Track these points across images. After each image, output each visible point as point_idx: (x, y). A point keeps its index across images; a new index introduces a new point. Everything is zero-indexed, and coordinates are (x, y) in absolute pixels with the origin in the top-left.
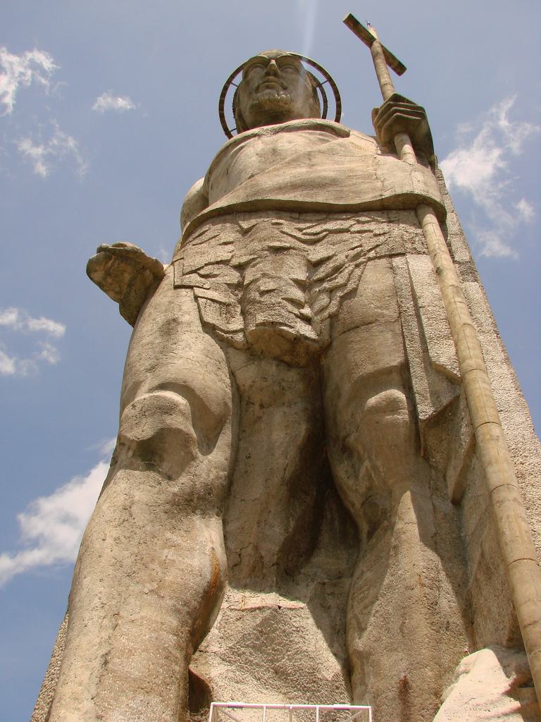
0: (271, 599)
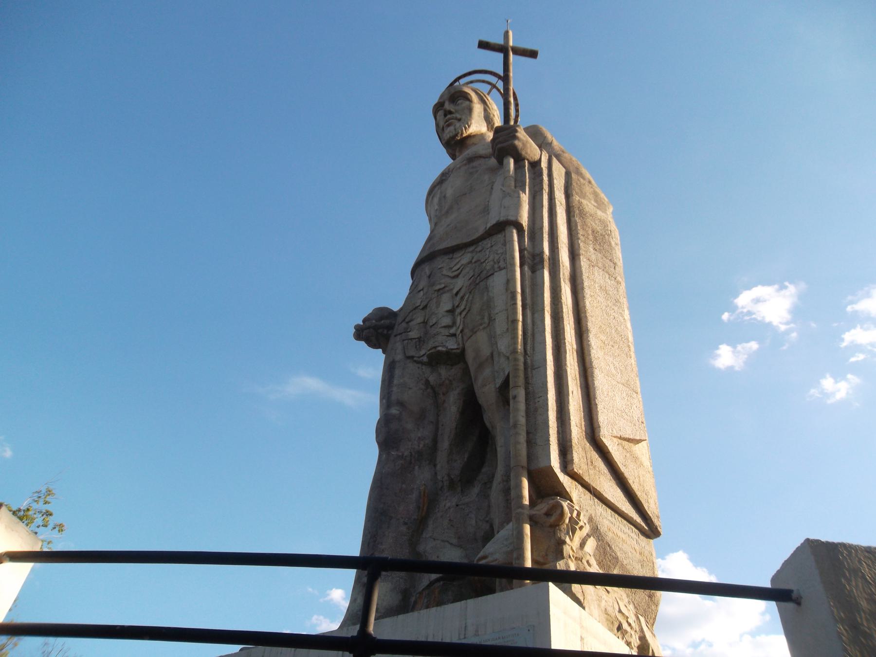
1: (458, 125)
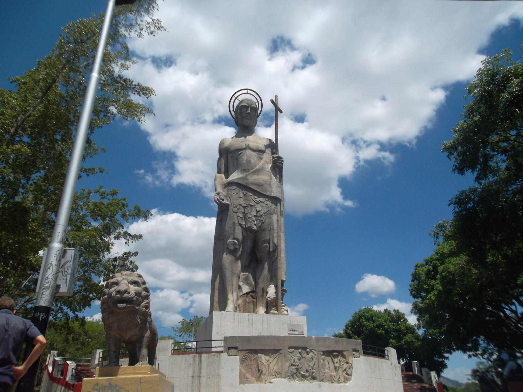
0: (247, 273)
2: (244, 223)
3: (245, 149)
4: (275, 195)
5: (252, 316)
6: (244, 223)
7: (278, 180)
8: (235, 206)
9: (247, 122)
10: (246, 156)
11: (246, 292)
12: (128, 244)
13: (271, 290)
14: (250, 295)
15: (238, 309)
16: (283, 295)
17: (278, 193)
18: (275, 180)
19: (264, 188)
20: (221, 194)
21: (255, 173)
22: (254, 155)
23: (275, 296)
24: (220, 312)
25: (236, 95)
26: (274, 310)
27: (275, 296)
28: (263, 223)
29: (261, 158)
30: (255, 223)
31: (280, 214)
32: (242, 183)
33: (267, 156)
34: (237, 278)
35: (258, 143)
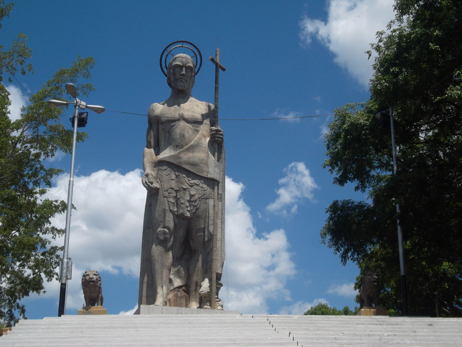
1: (185, 84)
2: (175, 210)
3: (178, 120)
4: (212, 176)
5: (182, 310)
6: (175, 210)
7: (216, 158)
8: (166, 190)
9: (182, 86)
10: (179, 129)
11: (178, 286)
12: (55, 239)
13: (205, 285)
14: (183, 289)
15: (168, 304)
16: (218, 289)
17: (215, 174)
18: (212, 159)
19: (200, 168)
20: (150, 176)
21: (188, 150)
22: (189, 127)
23: (209, 290)
24: (148, 306)
25: (169, 49)
26: (207, 305)
27: (209, 290)
28: (197, 209)
29: (197, 131)
30: (189, 209)
31: (217, 199)
32: (174, 162)
33: (205, 128)
34: (168, 271)
35: (194, 112)
